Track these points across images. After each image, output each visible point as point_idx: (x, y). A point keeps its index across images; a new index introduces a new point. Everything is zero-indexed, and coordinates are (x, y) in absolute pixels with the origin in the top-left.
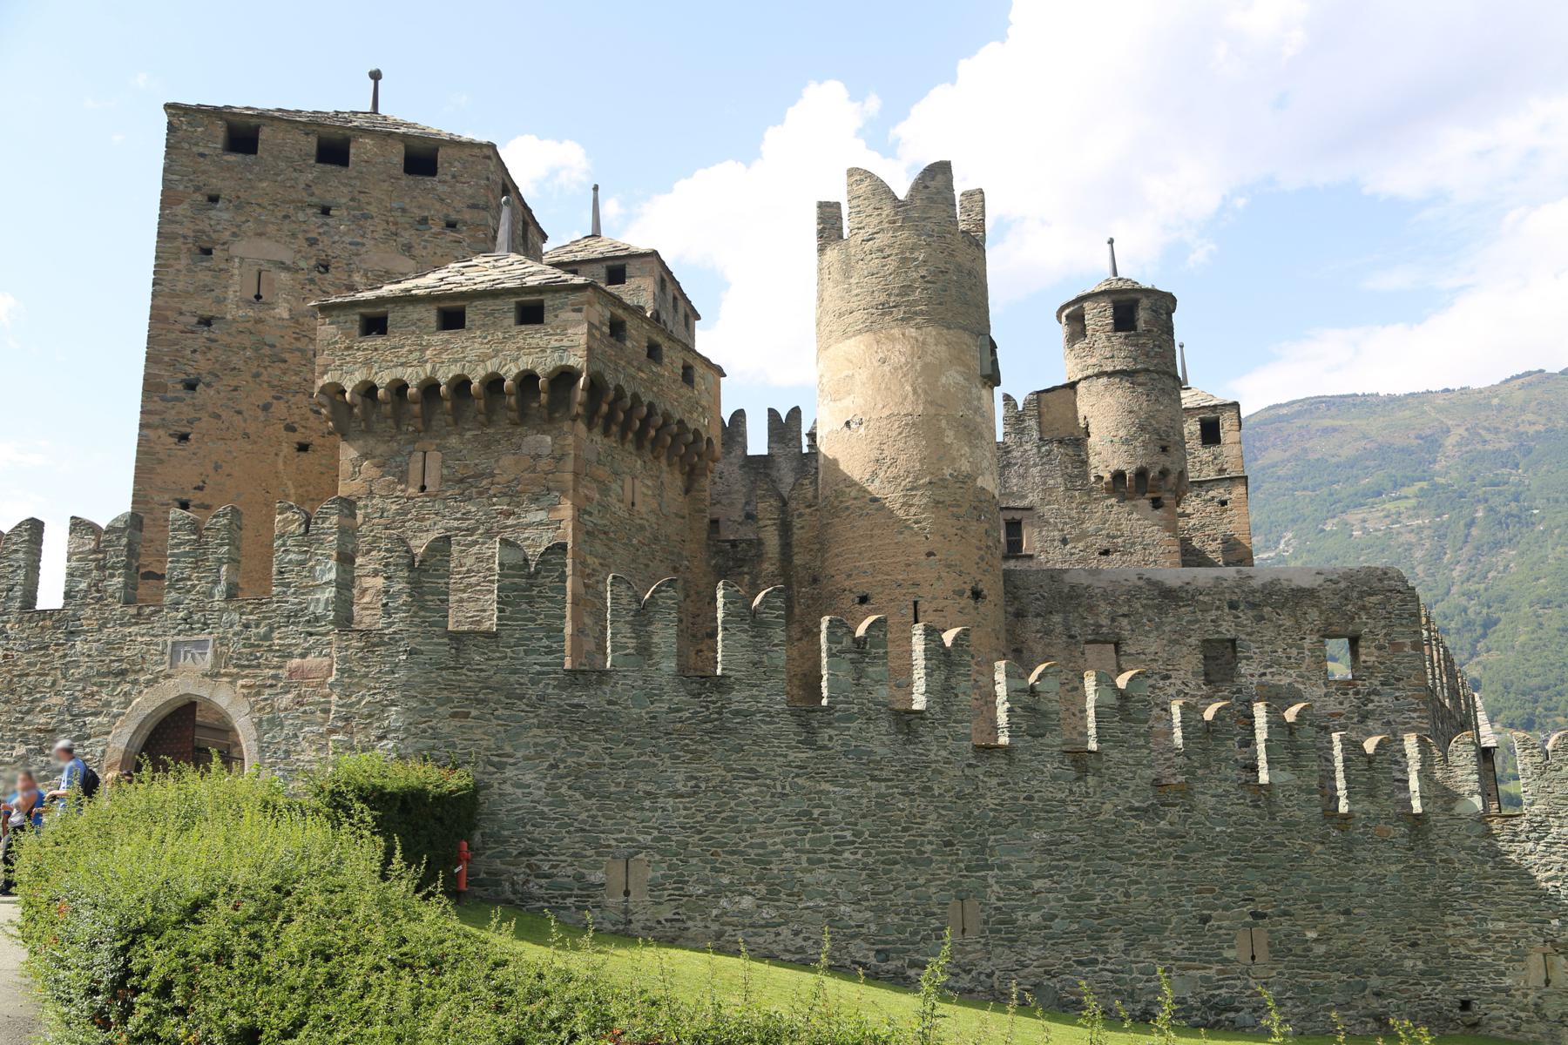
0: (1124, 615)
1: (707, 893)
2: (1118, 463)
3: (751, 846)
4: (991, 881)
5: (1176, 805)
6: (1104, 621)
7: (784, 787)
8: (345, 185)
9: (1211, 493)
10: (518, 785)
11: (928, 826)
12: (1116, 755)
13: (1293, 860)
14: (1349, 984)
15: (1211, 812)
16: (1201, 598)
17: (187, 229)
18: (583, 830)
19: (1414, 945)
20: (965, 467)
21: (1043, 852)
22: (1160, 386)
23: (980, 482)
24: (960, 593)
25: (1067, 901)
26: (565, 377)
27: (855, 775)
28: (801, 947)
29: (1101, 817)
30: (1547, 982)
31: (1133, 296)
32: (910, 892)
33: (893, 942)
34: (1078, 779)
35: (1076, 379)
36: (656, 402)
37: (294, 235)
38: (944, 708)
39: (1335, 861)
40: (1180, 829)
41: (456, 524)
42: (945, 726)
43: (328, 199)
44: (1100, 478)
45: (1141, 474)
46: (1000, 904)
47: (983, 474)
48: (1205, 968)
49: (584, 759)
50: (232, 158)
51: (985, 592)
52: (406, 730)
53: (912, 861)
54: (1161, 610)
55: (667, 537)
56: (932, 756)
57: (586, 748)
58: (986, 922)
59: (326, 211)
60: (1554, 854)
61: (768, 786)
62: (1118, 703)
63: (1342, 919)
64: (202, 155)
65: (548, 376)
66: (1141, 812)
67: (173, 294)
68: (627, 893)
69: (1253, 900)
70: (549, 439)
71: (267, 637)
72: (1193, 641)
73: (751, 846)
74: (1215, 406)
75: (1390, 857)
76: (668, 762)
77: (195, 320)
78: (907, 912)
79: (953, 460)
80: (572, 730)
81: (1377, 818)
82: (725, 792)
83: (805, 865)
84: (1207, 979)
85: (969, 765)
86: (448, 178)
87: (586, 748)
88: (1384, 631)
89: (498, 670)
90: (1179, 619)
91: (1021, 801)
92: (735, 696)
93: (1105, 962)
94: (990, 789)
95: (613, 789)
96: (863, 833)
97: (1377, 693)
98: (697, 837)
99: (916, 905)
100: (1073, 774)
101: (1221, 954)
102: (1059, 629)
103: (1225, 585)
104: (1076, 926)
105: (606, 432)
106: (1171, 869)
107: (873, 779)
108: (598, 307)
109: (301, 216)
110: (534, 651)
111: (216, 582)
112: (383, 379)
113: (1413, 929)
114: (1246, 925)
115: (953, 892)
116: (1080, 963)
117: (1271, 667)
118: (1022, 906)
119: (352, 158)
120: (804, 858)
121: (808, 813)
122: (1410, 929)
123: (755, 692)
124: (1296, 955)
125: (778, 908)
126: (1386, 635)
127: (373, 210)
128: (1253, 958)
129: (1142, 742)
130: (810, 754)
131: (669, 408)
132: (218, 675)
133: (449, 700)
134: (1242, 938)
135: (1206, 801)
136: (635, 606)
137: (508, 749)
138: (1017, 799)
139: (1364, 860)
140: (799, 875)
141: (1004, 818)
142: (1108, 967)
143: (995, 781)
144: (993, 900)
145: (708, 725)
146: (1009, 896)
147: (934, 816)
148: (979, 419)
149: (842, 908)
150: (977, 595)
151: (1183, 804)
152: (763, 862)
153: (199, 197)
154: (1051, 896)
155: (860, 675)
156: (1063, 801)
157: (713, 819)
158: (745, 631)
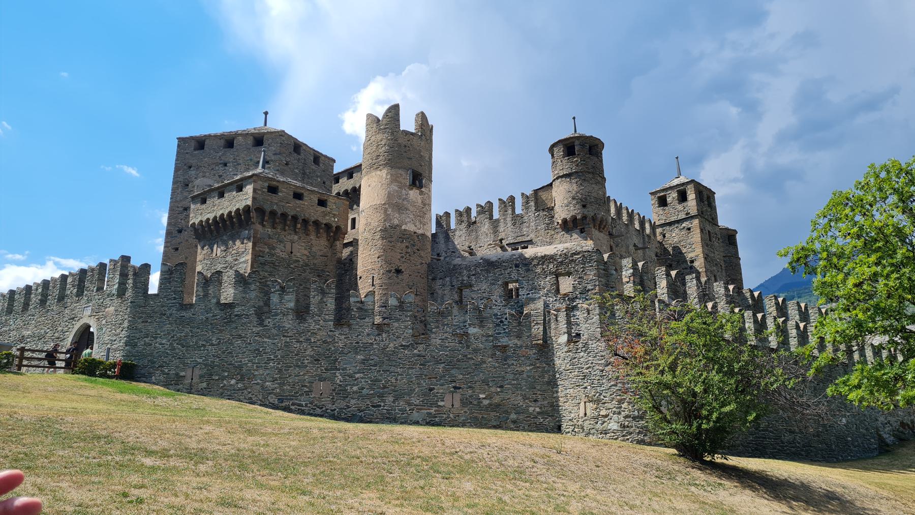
0: (473, 275)
1: (219, 379)
2: (564, 216)
3: (236, 362)
4: (337, 374)
5: (422, 344)
6: (465, 278)
7: (250, 341)
8: (232, 154)
9: (684, 225)
10: (160, 344)
11: (307, 353)
12: (396, 325)
13: (476, 365)
14: (499, 417)
15: (438, 346)
16: (504, 264)
17: (181, 179)
18: (180, 358)
19: (535, 401)
20: (396, 222)
21: (360, 363)
22: (583, 178)
23: (403, 227)
24: (390, 271)
25: (369, 382)
26: (247, 209)
27: (277, 335)
28: (251, 398)
29: (388, 349)
30: (585, 414)
31: (571, 140)
32: (296, 378)
33: (287, 396)
34: (379, 335)
35: (551, 181)
36: (298, 214)
37: (214, 175)
38: (319, 310)
39: (497, 365)
40: (423, 353)
41: (223, 265)
42: (319, 316)
43: (226, 160)
44: (558, 223)
45: (574, 219)
46: (341, 383)
47: (406, 224)
48: (429, 409)
49: (183, 334)
50: (196, 152)
51: (403, 270)
52: (128, 328)
53: (298, 366)
54: (488, 271)
55: (314, 264)
56: (312, 328)
57: (184, 330)
58: (334, 390)
59: (225, 165)
60: (590, 356)
61: (244, 341)
62: (398, 304)
63: (499, 390)
64: (187, 153)
65: (243, 209)
66: (404, 347)
67: (176, 201)
68: (192, 379)
69: (455, 382)
70: (247, 232)
71: (102, 303)
72: (500, 283)
73: (236, 362)
74: (683, 184)
75: (526, 363)
76: (211, 334)
77: (182, 209)
78: (294, 385)
79: (391, 220)
80: (180, 325)
81: (521, 346)
82: (230, 343)
83: (255, 368)
84: (431, 413)
85: (331, 331)
86: (267, 146)
87: (184, 330)
88: (582, 270)
89: (158, 306)
90: (495, 274)
91: (354, 344)
92: (236, 310)
93: (384, 406)
94: (341, 340)
95: (191, 344)
96: (278, 356)
97: (576, 298)
98: (218, 359)
99: (298, 383)
100: (376, 332)
101: (437, 404)
102: (448, 283)
103: (514, 257)
104: (372, 392)
105: (274, 228)
106: (418, 369)
107: (284, 336)
108: (260, 182)
109: (217, 168)
110: (170, 299)
111: (94, 287)
112: (204, 219)
113: (536, 394)
114: (451, 392)
115: (317, 378)
116: (372, 406)
117: (532, 290)
118: (350, 384)
119: (235, 145)
120: (255, 365)
121: (258, 350)
122: (534, 394)
123: (243, 308)
124: (474, 405)
125: (244, 384)
126: (582, 271)
127: (241, 162)
128: (453, 405)
129: (409, 319)
130: (261, 328)
131: (307, 216)
132: (91, 316)
133: (141, 317)
134: (448, 397)
135: (436, 341)
136: (204, 281)
137: (159, 332)
138: (352, 343)
139: (513, 364)
140: (252, 372)
141: (346, 351)
142: (385, 408)
143: (343, 337)
144: (338, 382)
145: (226, 320)
146: (345, 380)
147: (311, 350)
148: (405, 203)
149: (267, 383)
150: (398, 271)
151: (426, 343)
152: (240, 367)
153: (185, 167)
154: (363, 380)
155: (281, 298)
156: (372, 344)
157: (224, 353)
158: (241, 287)
